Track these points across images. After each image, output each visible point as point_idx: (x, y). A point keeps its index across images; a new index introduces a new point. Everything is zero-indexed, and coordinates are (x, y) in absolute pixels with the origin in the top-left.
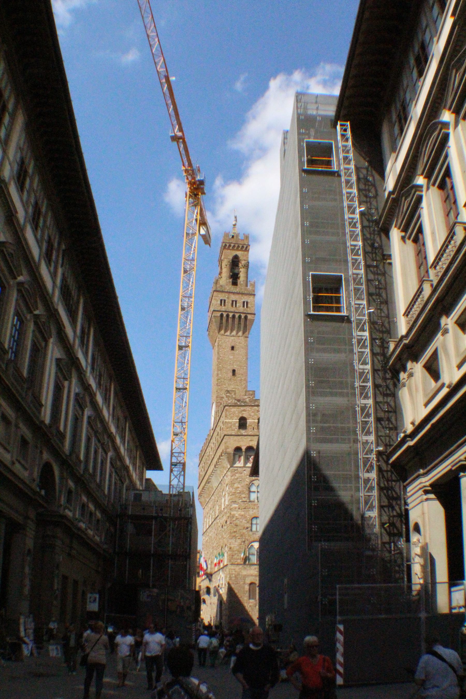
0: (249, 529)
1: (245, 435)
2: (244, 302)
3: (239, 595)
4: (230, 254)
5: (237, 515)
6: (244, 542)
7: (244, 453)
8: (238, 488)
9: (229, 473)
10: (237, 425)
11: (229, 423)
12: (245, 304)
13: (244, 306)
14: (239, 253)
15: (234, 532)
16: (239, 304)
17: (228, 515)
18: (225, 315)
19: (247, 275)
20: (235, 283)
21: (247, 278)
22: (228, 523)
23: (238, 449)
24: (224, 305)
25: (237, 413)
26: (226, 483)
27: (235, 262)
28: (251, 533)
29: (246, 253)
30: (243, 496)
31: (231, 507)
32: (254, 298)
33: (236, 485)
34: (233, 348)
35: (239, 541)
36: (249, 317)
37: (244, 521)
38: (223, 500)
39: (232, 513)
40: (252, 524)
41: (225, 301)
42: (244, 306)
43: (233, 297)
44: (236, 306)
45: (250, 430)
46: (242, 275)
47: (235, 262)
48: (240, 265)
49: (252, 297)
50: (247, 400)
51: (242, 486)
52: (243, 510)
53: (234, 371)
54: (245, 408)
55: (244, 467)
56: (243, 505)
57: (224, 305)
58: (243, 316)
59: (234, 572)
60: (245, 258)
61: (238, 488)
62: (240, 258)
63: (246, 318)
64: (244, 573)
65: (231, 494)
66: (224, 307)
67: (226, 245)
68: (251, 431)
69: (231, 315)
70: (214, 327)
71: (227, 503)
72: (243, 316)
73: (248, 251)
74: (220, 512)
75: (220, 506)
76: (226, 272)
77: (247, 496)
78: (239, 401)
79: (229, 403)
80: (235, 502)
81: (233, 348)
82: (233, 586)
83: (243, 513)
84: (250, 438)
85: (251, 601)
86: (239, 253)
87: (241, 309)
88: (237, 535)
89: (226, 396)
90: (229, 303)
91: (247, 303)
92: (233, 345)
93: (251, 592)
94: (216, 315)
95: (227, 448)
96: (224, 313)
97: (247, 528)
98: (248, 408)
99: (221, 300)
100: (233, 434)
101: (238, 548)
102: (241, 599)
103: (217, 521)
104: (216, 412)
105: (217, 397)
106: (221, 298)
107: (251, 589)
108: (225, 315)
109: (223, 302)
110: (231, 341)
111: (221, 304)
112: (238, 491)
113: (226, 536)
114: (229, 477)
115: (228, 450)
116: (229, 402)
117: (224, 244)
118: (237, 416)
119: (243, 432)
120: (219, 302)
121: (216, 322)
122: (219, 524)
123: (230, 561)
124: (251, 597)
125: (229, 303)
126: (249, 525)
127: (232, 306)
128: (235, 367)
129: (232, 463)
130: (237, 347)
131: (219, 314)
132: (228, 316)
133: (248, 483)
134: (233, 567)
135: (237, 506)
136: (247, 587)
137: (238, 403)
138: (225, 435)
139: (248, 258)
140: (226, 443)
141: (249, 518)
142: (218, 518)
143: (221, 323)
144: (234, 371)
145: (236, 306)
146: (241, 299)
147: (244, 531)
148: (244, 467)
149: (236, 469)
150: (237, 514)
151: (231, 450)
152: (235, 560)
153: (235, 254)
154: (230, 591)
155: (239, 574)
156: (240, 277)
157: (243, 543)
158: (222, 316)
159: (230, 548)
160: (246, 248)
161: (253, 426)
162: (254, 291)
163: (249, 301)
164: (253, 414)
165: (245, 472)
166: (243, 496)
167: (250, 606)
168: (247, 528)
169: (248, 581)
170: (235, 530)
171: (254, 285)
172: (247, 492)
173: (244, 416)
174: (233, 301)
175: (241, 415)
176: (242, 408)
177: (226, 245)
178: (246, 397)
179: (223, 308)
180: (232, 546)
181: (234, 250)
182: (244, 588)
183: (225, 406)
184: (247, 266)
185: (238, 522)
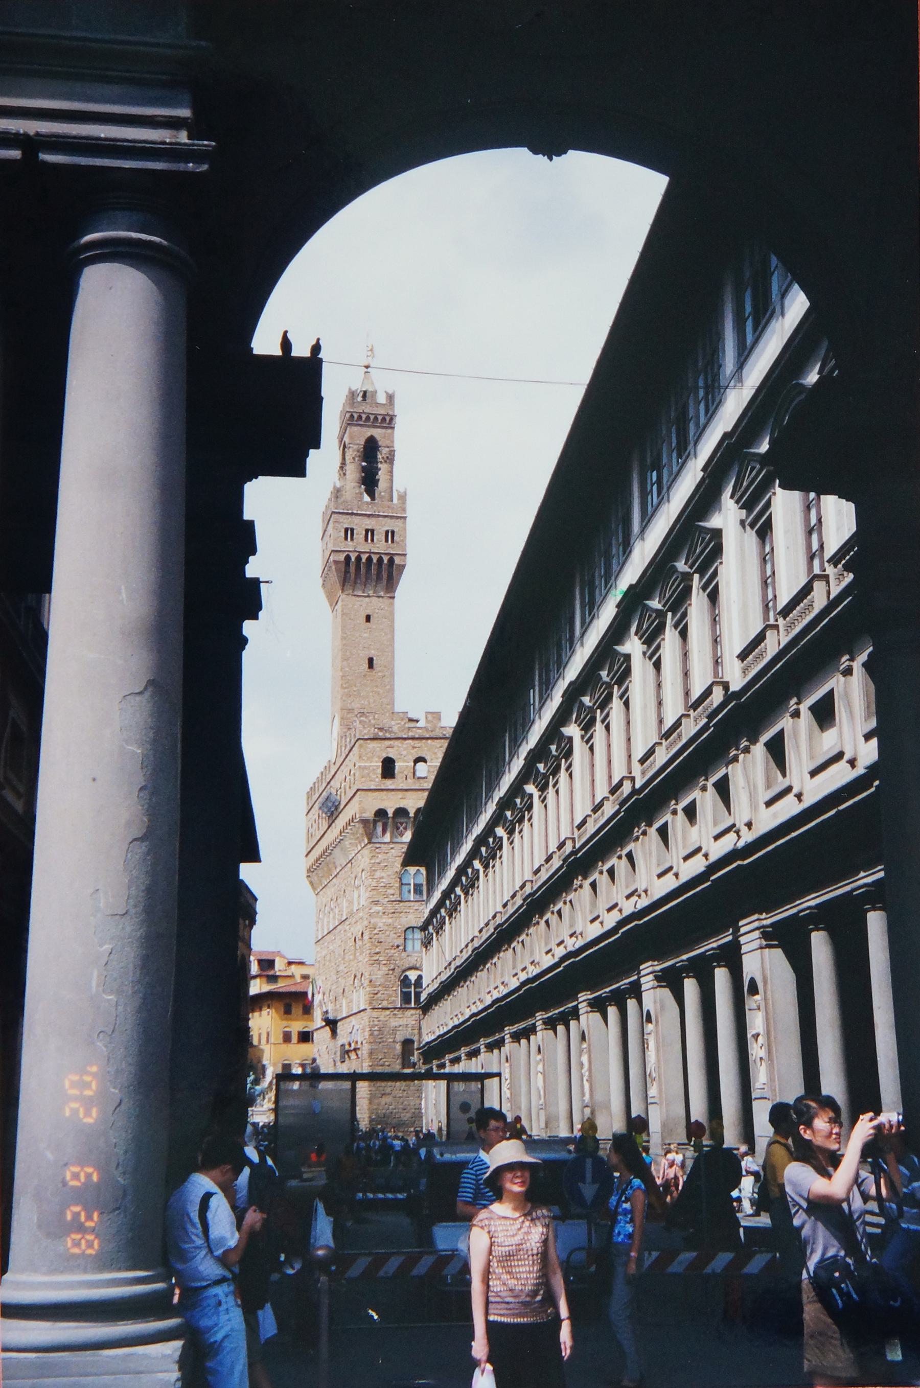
0: (401, 948)
1: (393, 790)
2: (387, 532)
4: (361, 434)
5: (380, 925)
6: (393, 970)
7: (390, 820)
8: (382, 878)
9: (366, 852)
10: (380, 771)
11: (365, 767)
12: (390, 535)
13: (387, 541)
14: (377, 433)
15: (377, 953)
16: (379, 536)
17: (366, 923)
18: (353, 559)
19: (392, 476)
20: (371, 493)
21: (391, 480)
22: (366, 937)
23: (381, 814)
24: (352, 539)
25: (381, 751)
26: (361, 867)
27: (370, 449)
28: (404, 954)
29: (389, 431)
30: (391, 891)
31: (372, 911)
32: (405, 523)
33: (378, 874)
34: (368, 618)
35: (385, 969)
36: (397, 560)
37: (392, 935)
38: (356, 894)
39: (372, 921)
40: (405, 939)
41: (352, 530)
42: (387, 541)
43: (369, 523)
44: (372, 540)
45: (400, 780)
46: (382, 475)
47: (370, 449)
48: (379, 456)
49: (399, 523)
50: (395, 729)
51: (389, 876)
52: (390, 916)
53: (371, 661)
54: (391, 742)
55: (391, 842)
56: (390, 908)
57: (352, 539)
58: (386, 559)
59: (376, 1023)
60: (388, 443)
61: (382, 878)
62: (380, 443)
63: (391, 561)
64: (394, 1023)
65: (369, 889)
66: (351, 543)
67: (352, 416)
68: (403, 782)
69: (364, 557)
70: (334, 578)
71: (362, 902)
72: (386, 559)
73: (393, 428)
74: (351, 914)
75: (351, 902)
76: (353, 472)
77: (398, 892)
78: (381, 729)
79: (365, 734)
80: (376, 903)
81: (368, 618)
83: (390, 921)
84: (400, 794)
86: (377, 433)
87: (380, 546)
88: (381, 959)
89: (360, 722)
90: (359, 535)
91: (393, 532)
92: (368, 612)
94: (337, 559)
95: (363, 810)
96: (351, 554)
97: (398, 946)
98: (397, 743)
99: (346, 530)
100: (372, 787)
101: (382, 980)
103: (345, 926)
104: (342, 737)
105: (342, 709)
106: (346, 526)
108: (353, 559)
109: (349, 533)
110: (364, 605)
111: (346, 538)
112: (382, 884)
113: (364, 958)
114: (368, 860)
115: (364, 815)
116: (366, 731)
117: (348, 415)
118: (379, 757)
119: (389, 784)
120: (342, 534)
121: (337, 570)
122: (349, 935)
123: (370, 1003)
125: (359, 535)
126: (400, 941)
127: (366, 540)
128: (372, 653)
129: (370, 836)
130: (375, 615)
131: (342, 557)
132: (359, 559)
133: (398, 870)
134: (375, 1014)
135: (381, 908)
136: (398, 1047)
137: (381, 734)
138: (358, 790)
139: (393, 442)
140: (360, 802)
141: (401, 928)
142: (347, 923)
143: (347, 572)
144: (371, 661)
145: (372, 540)
146: (381, 526)
147: (393, 951)
148: (391, 842)
149: (378, 846)
150: (381, 922)
151: (369, 815)
153: (369, 434)
155: (385, 1026)
156: (378, 480)
157: (391, 972)
158: (348, 558)
159: (371, 981)
160: (388, 422)
161: (406, 773)
162: (404, 510)
163: (396, 530)
164: (404, 753)
165: (393, 851)
166: (391, 891)
168: (398, 946)
169: (400, 1037)
170: (377, 950)
171: (403, 497)
172: (397, 885)
173: (391, 755)
174: (367, 531)
175: (384, 755)
176: (387, 743)
177: (352, 416)
178: (393, 723)
179: (349, 546)
180: (373, 978)
181: (368, 426)
183: (359, 739)
184: (390, 460)
185: (382, 937)
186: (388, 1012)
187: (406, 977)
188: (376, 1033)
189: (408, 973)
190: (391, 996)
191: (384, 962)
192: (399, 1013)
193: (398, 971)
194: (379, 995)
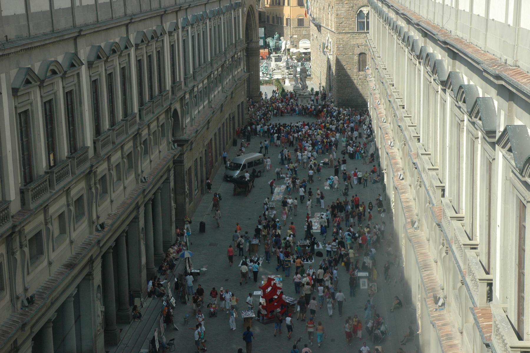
3: (347, 67)
59: (341, 42)
82: (340, 58)
85: (361, 73)
93: (361, 63)
101: (345, 14)
102: (349, 72)
107: (361, 59)
123: (337, 29)
124: (361, 68)
136: (356, 58)
152: (343, 29)
154: (338, 62)
159: (337, 15)
167: (360, 79)
169: (357, 51)
182: (353, 59)
186: (349, 35)
187: (361, 11)
188: (341, 49)
189: (362, 9)
190: (351, 25)
191: (346, 2)
192: (357, 36)
193: (356, 7)
194: (343, 24)
